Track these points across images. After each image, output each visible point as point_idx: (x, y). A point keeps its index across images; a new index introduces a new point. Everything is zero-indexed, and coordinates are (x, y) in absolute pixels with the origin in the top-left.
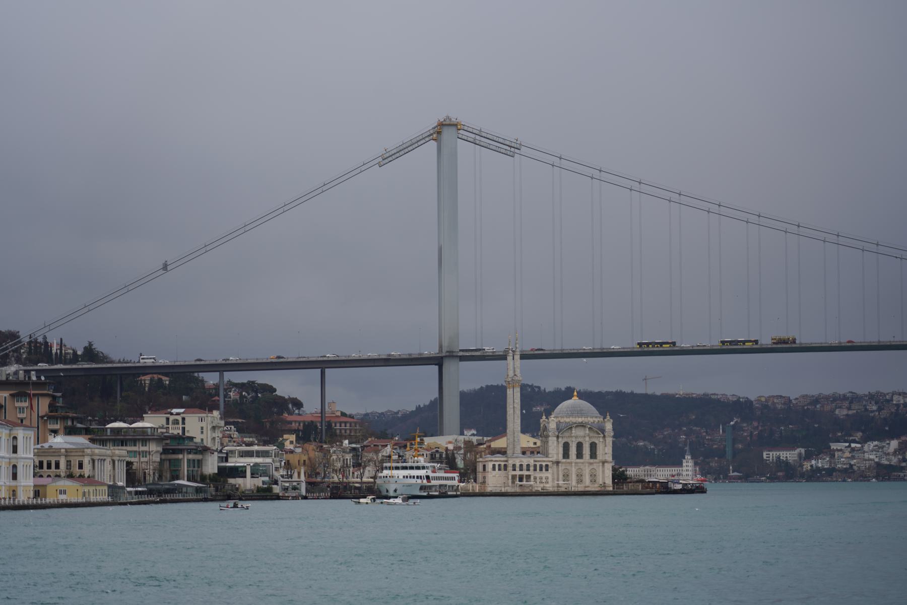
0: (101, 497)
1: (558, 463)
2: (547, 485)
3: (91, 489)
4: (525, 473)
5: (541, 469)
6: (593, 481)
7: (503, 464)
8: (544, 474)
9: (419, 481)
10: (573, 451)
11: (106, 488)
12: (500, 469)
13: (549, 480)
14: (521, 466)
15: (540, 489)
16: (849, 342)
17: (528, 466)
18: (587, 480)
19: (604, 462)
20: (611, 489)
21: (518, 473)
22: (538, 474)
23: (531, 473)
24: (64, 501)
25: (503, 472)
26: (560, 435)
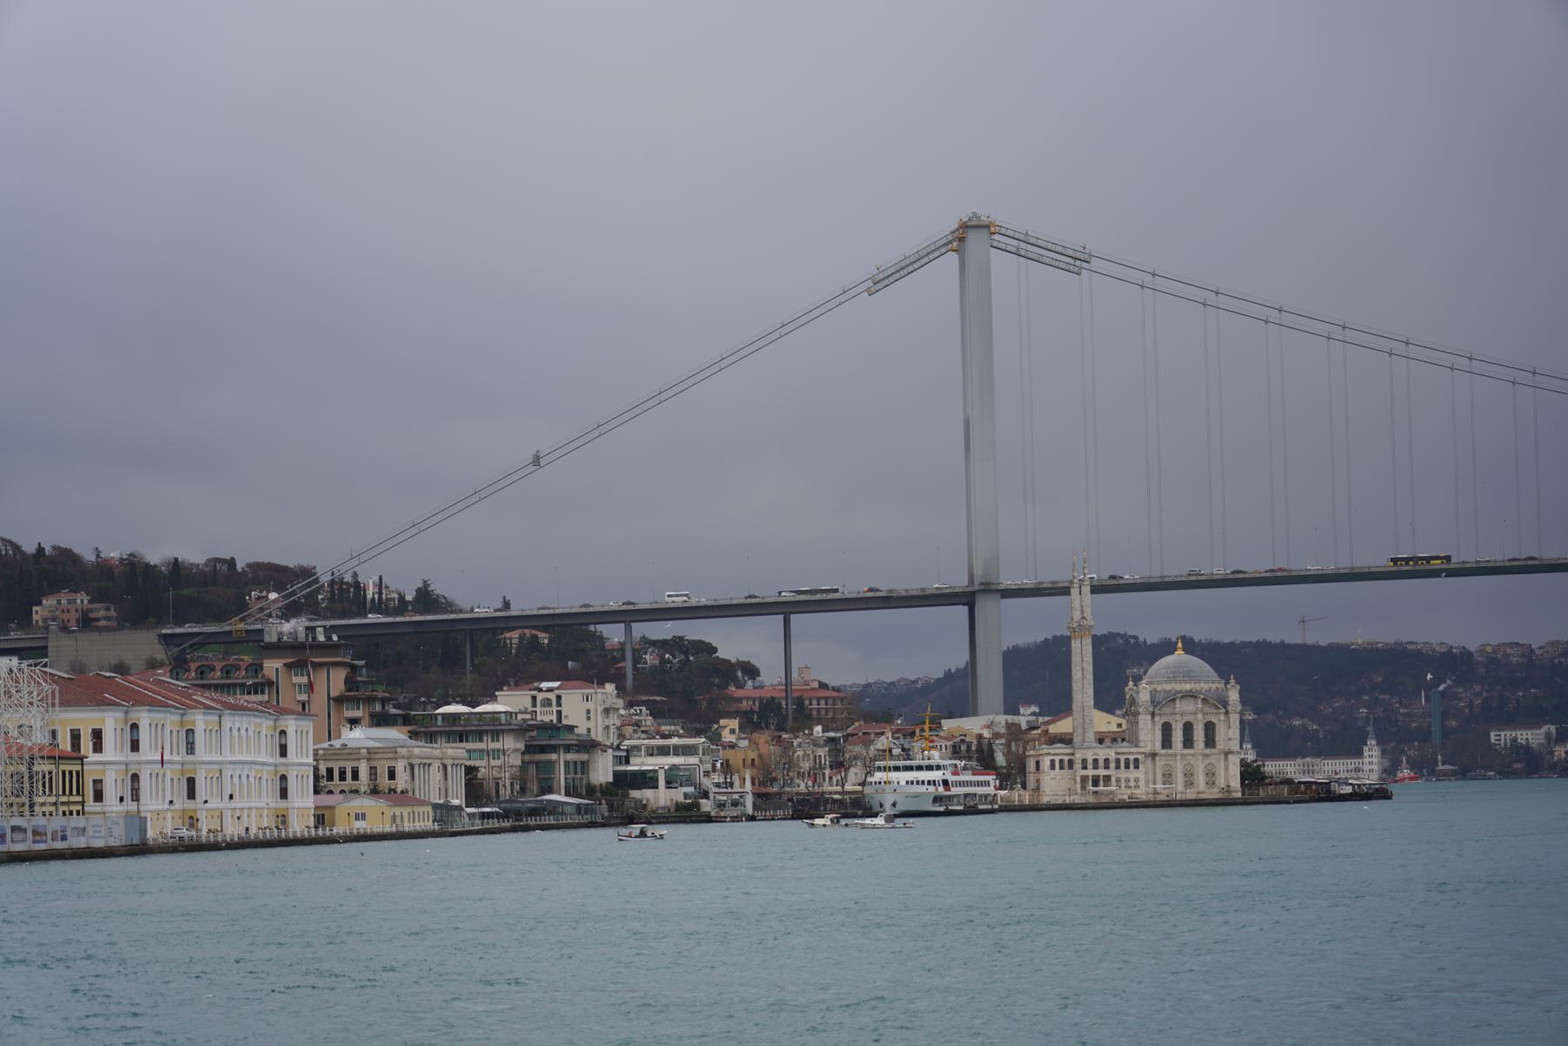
0: (422, 824)
1: (1153, 755)
2: (1138, 791)
3: (406, 811)
4: (1102, 772)
5: (1127, 767)
6: (1211, 783)
7: (1066, 758)
8: (1132, 774)
9: (932, 789)
10: (1178, 736)
11: (430, 809)
12: (1061, 768)
13: (1142, 782)
14: (1096, 761)
15: (1126, 797)
16: (870, 590)
18: (1201, 781)
19: (1227, 753)
20: (1239, 795)
21: (1090, 772)
22: (1123, 774)
23: (1111, 772)
24: (362, 831)
25: (1066, 772)
26: (1157, 712)
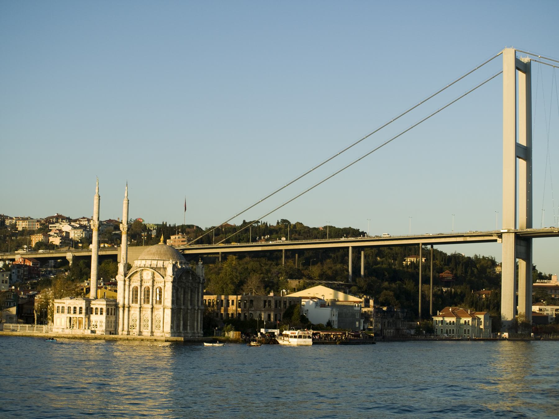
21: (72, 315)
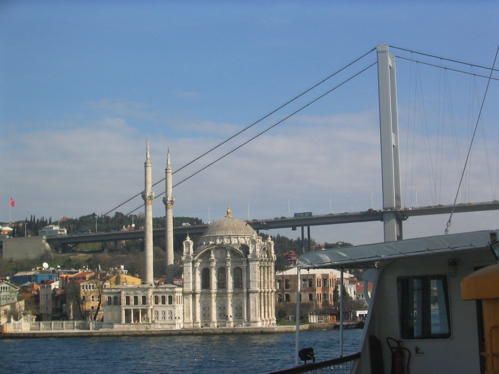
4: (140, 307)
14: (136, 298)
17: (144, 298)
